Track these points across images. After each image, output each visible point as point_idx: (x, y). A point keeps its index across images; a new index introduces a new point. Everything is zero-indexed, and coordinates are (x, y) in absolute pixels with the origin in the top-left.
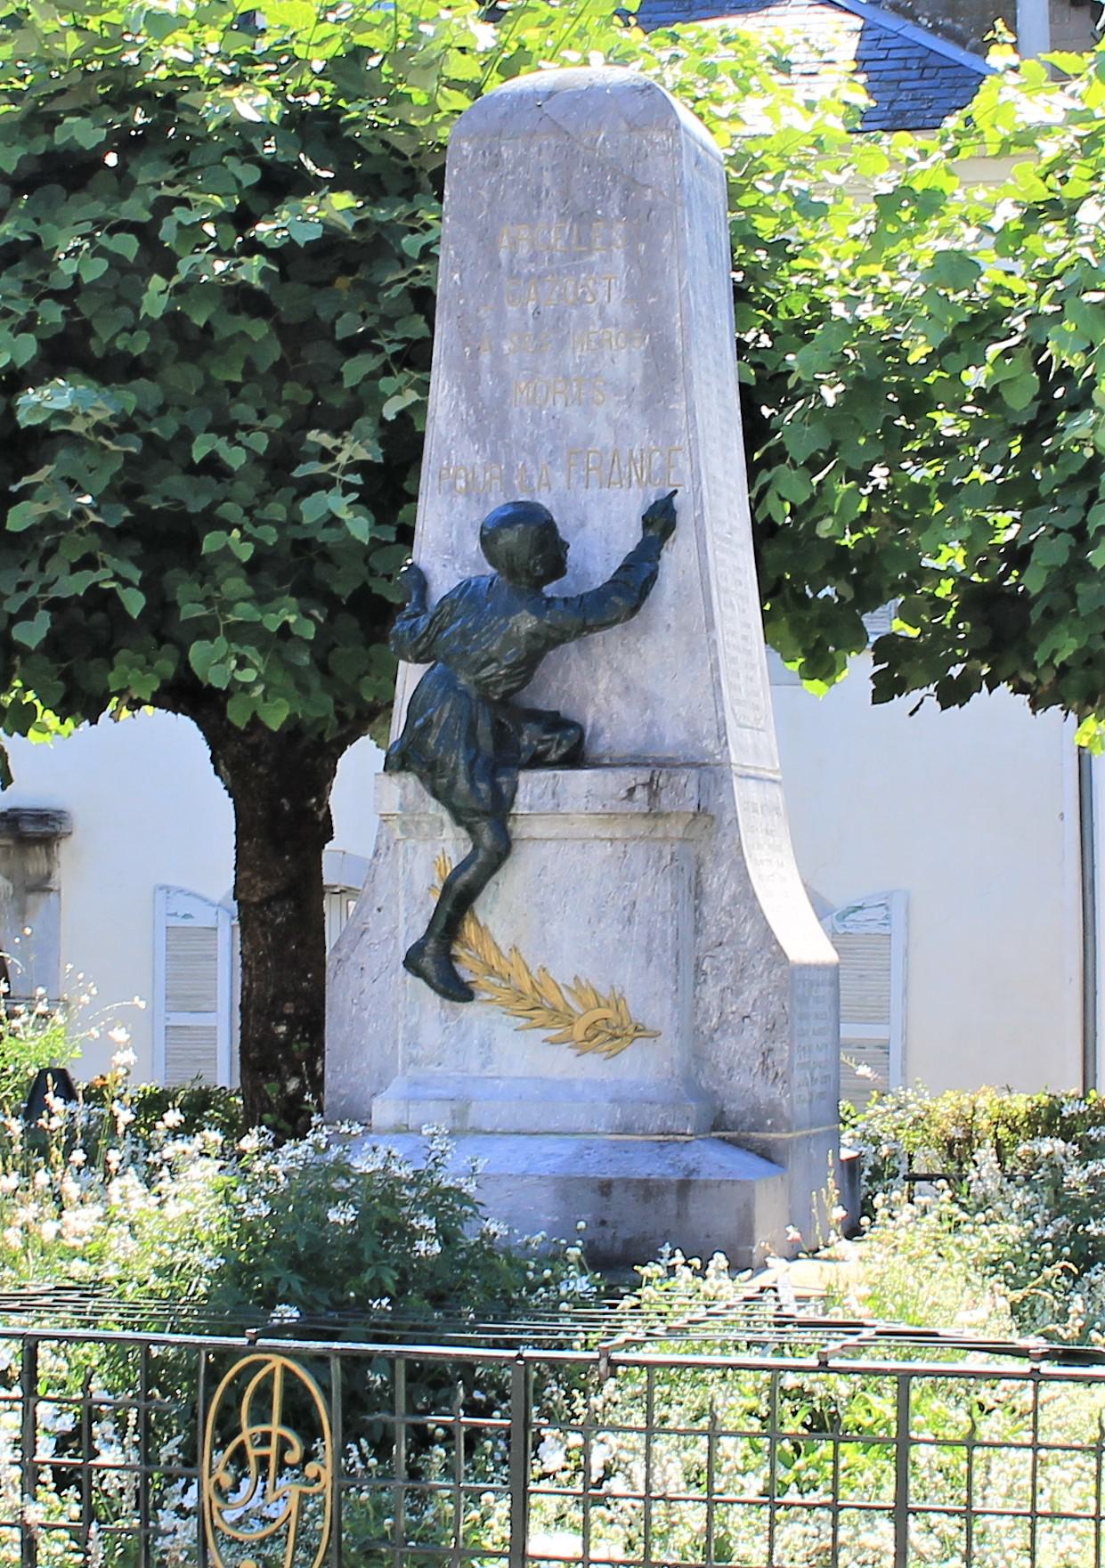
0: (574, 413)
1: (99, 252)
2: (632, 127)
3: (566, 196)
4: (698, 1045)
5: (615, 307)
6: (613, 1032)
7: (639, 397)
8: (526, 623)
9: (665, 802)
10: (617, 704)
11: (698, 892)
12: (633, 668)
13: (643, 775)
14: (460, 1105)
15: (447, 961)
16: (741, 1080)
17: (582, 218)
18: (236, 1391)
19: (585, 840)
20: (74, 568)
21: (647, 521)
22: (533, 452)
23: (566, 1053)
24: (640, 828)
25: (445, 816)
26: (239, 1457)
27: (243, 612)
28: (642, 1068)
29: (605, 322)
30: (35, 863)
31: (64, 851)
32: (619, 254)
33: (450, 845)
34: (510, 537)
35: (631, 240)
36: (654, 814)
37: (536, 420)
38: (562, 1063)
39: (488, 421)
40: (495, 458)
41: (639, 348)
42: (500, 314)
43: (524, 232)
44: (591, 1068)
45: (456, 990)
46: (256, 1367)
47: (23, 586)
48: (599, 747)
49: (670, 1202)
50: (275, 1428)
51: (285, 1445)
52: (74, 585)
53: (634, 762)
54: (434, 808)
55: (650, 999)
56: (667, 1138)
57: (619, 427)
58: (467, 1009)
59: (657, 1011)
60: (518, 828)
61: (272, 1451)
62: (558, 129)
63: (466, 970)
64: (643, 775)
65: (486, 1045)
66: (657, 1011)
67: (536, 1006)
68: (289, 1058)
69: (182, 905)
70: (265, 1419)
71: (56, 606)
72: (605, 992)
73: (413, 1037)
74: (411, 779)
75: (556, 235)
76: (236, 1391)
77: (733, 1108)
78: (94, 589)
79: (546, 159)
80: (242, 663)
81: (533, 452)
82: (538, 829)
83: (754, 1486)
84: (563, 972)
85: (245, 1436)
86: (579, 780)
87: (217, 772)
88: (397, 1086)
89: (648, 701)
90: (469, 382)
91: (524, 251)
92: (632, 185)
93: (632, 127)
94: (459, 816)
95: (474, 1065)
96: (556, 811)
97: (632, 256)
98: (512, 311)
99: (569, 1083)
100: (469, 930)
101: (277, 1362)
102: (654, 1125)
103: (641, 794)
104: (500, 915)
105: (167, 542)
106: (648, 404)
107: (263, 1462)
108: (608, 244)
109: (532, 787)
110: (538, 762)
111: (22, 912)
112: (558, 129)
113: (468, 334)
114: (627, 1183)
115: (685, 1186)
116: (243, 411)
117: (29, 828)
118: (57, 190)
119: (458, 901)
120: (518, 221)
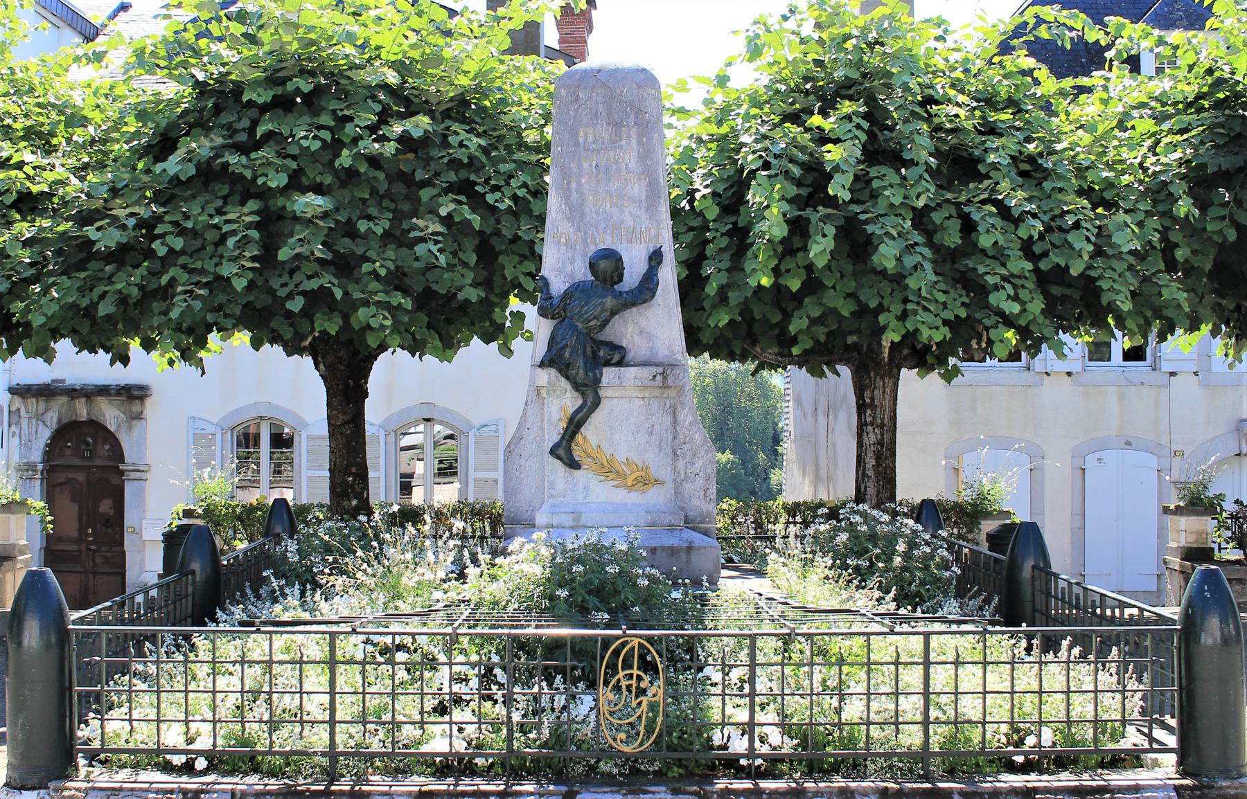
0: (615, 211)
1: (315, 137)
2: (639, 87)
3: (609, 115)
4: (678, 485)
5: (632, 165)
6: (645, 481)
7: (644, 204)
8: (609, 302)
9: (670, 381)
10: (637, 339)
11: (675, 421)
12: (644, 323)
13: (660, 370)
14: (577, 515)
15: (569, 451)
16: (694, 502)
17: (617, 125)
18: (617, 653)
19: (631, 398)
20: (309, 277)
21: (650, 259)
22: (596, 227)
23: (622, 492)
24: (657, 392)
25: (569, 387)
26: (617, 688)
27: (380, 297)
28: (656, 497)
29: (629, 172)
30: (136, 407)
31: (148, 402)
32: (634, 142)
33: (567, 400)
34: (603, 265)
35: (639, 136)
36: (665, 387)
37: (597, 214)
38: (621, 496)
39: (575, 213)
40: (579, 229)
41: (644, 184)
42: (580, 166)
43: (590, 130)
44: (635, 497)
45: (573, 465)
46: (623, 645)
47: (285, 285)
48: (629, 357)
49: (683, 556)
50: (635, 672)
51: (639, 678)
52: (313, 285)
53: (646, 364)
54: (564, 383)
55: (659, 465)
56: (672, 528)
57: (635, 218)
58: (577, 473)
59: (665, 473)
60: (602, 393)
61: (634, 682)
62: (604, 85)
63: (577, 453)
64: (660, 370)
65: (586, 488)
66: (665, 473)
67: (609, 470)
68: (353, 490)
69: (201, 425)
70: (631, 668)
71: (304, 294)
72: (640, 465)
73: (552, 487)
74: (553, 371)
75: (605, 132)
76: (617, 653)
77: (692, 514)
78: (321, 287)
79: (600, 99)
80: (385, 318)
81: (596, 227)
82: (610, 393)
83: (861, 688)
84: (621, 456)
85: (621, 674)
86: (630, 372)
87: (317, 367)
88: (546, 507)
89: (650, 338)
90: (566, 195)
91: (591, 139)
92: (639, 112)
93: (639, 87)
94: (576, 387)
95: (580, 498)
96: (620, 386)
97: (640, 143)
98: (585, 165)
99: (625, 505)
100: (579, 437)
101: (636, 640)
102: (666, 522)
103: (659, 378)
104: (591, 432)
105: (344, 266)
106: (648, 208)
107: (629, 688)
108: (629, 137)
109: (609, 374)
110: (608, 363)
111: (130, 428)
112: (604, 85)
113: (565, 174)
114: (663, 548)
115: (689, 549)
116: (373, 211)
117: (136, 393)
118: (280, 112)
119: (575, 425)
120: (587, 125)
